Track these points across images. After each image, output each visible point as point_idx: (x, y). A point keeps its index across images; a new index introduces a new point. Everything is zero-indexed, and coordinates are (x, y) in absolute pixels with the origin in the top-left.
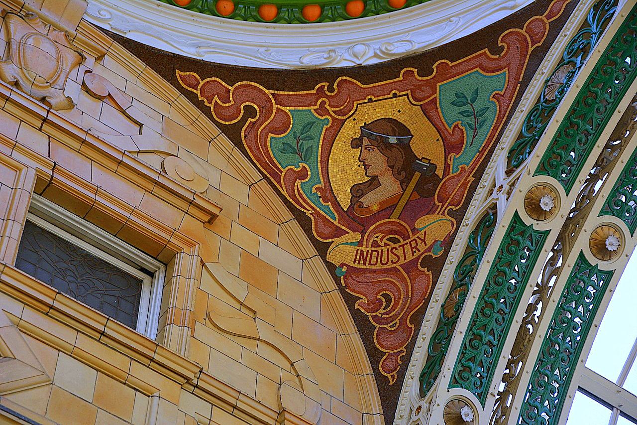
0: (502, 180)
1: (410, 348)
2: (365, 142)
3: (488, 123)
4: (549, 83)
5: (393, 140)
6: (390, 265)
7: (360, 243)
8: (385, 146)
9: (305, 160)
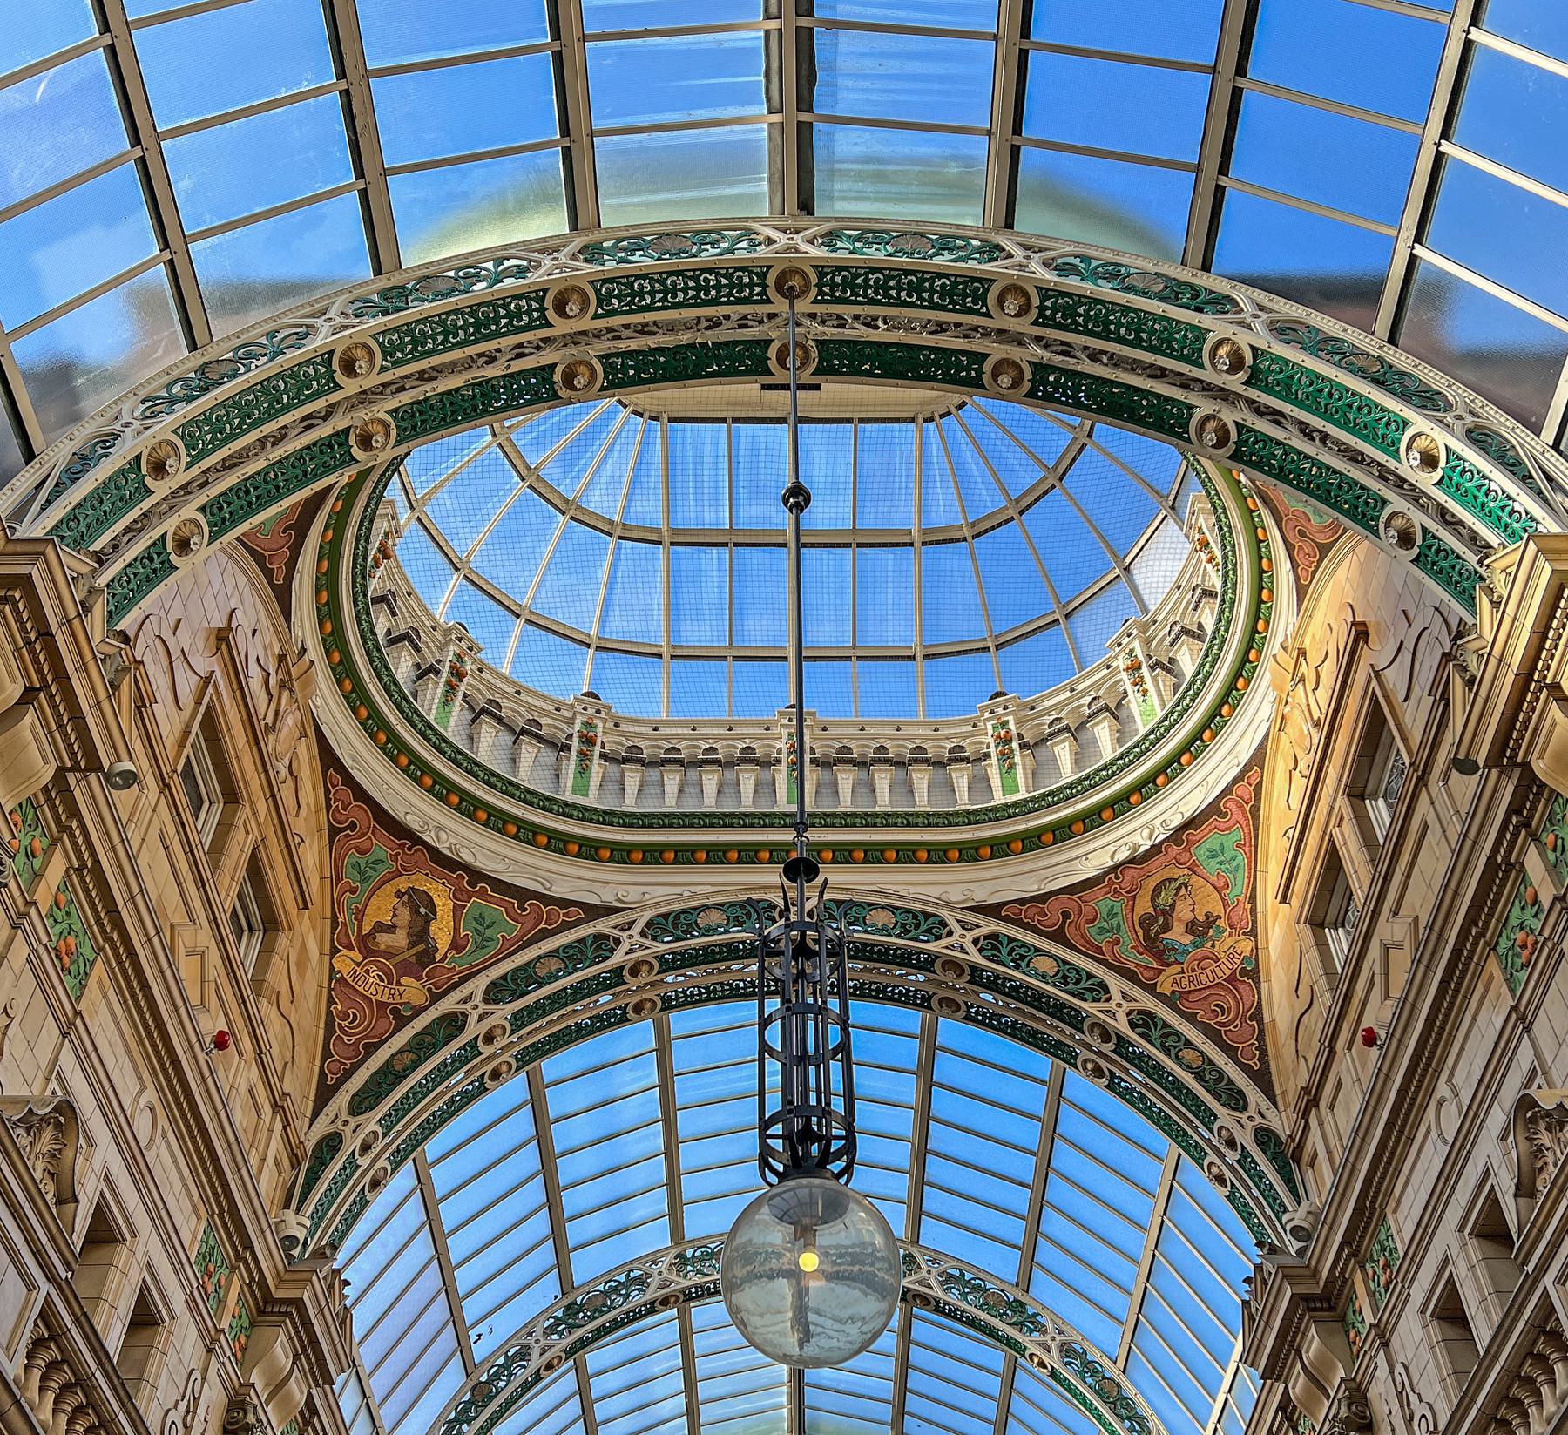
1: (356, 1067)
2: (405, 898)
3: (487, 950)
5: (423, 910)
6: (368, 994)
7: (358, 964)
8: (415, 911)
9: (362, 882)
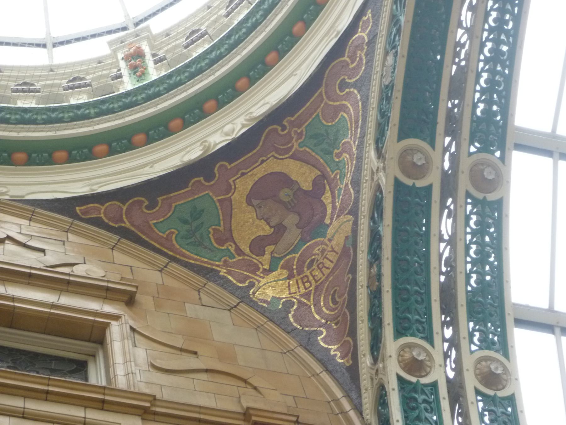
0: (376, 164)
4: (384, 74)
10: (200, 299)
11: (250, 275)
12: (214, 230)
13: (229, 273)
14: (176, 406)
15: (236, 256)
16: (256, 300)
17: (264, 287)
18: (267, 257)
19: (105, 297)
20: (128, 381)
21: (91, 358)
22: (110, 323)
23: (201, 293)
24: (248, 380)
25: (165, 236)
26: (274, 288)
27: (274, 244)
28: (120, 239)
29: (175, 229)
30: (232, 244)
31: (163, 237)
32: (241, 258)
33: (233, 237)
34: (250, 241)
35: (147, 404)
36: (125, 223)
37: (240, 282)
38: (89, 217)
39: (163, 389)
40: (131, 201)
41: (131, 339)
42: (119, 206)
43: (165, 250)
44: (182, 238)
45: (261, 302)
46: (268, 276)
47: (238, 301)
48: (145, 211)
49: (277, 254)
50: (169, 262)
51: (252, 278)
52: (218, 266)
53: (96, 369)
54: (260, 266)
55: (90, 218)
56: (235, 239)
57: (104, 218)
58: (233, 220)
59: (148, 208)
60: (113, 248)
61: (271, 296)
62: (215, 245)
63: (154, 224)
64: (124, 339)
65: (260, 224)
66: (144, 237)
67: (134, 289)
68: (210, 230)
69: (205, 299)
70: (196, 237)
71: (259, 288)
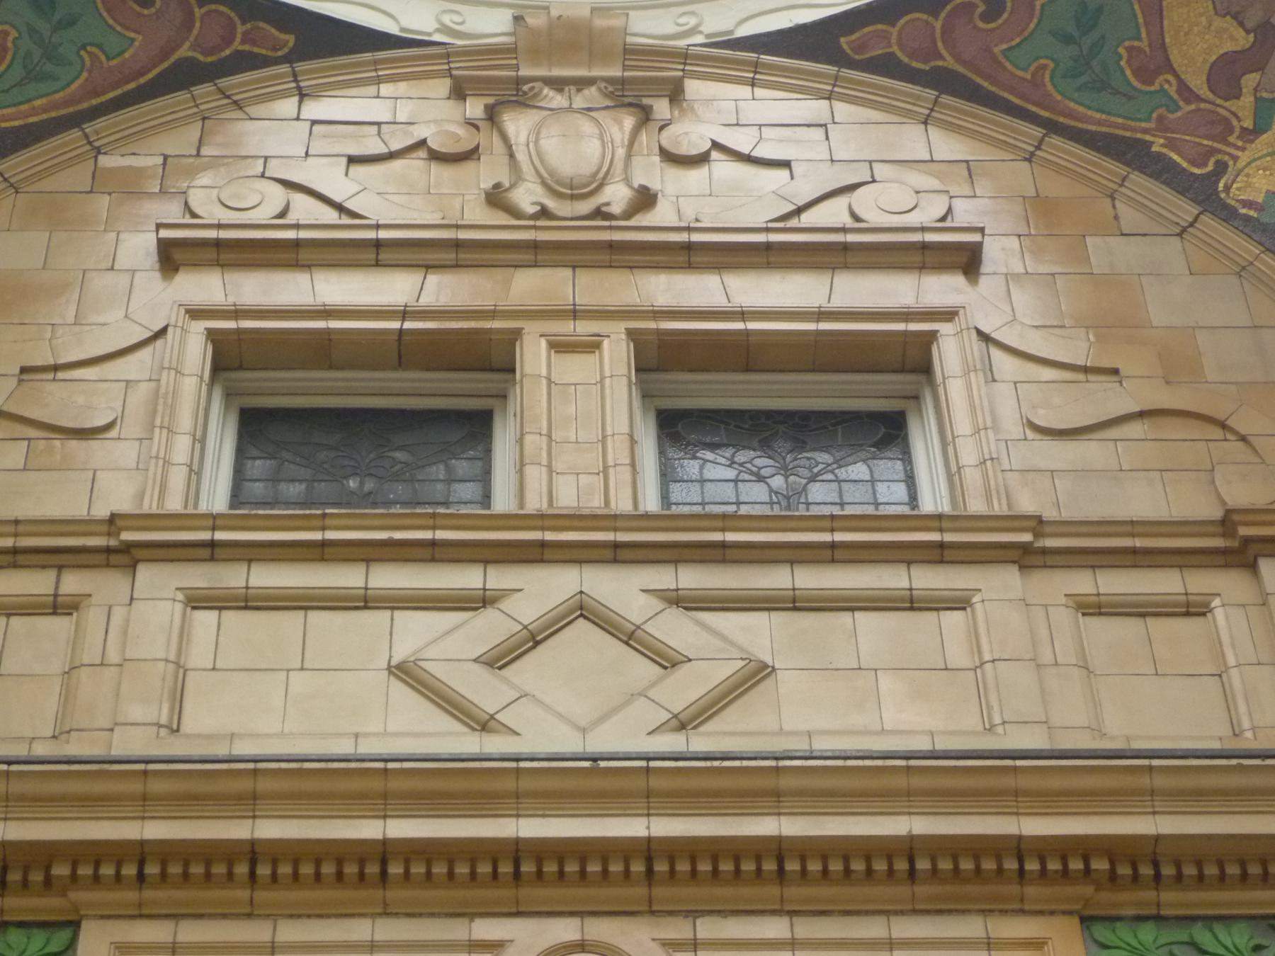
10: (1116, 217)
11: (1216, 145)
12: (1130, 49)
13: (1171, 144)
14: (1084, 529)
15: (1181, 103)
16: (1233, 203)
17: (1246, 171)
18: (1247, 100)
19: (922, 265)
20: (985, 476)
21: (912, 403)
22: (938, 331)
23: (1117, 202)
24: (1228, 422)
25: (1029, 77)
26: (1268, 173)
27: (1256, 71)
28: (938, 97)
29: (1047, 57)
30: (1170, 77)
31: (1025, 80)
32: (1193, 107)
33: (1169, 60)
34: (1208, 66)
35: (1026, 537)
36: (944, 60)
37: (1198, 166)
38: (867, 56)
39: (1056, 481)
40: (948, 8)
41: (984, 371)
42: (927, 23)
43: (1034, 109)
44: (1064, 77)
45: (1244, 207)
46: (1253, 145)
47: (1196, 212)
48: (981, 25)
49: (1266, 91)
50: (1045, 135)
51: (1219, 151)
52: (1146, 131)
53: (924, 427)
54: (1235, 122)
55: (872, 58)
56: (1175, 66)
57: (899, 54)
58: (1166, 22)
59: (986, 17)
60: (927, 119)
61: (1264, 191)
62: (1135, 83)
63: (1003, 52)
64: (969, 372)
65: (1225, 25)
66: (986, 84)
67: (976, 237)
68: (1121, 50)
69: (1129, 217)
70: (1093, 72)
71: (1238, 175)
